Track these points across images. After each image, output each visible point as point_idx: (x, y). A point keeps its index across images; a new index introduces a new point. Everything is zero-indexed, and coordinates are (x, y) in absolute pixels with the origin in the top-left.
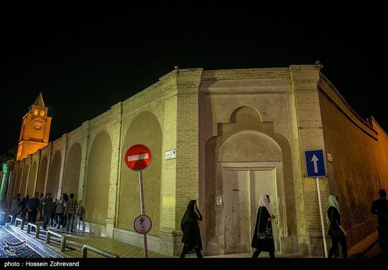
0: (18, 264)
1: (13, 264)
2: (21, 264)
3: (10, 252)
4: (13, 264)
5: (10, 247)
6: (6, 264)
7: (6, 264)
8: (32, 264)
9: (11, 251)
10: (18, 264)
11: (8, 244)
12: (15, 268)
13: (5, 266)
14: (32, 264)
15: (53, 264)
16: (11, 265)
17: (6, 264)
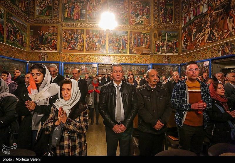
0: (11, 160)
1: (8, 160)
2: (13, 160)
3: (7, 153)
4: (8, 160)
5: (6, 149)
6: (4, 160)
7: (4, 160)
8: (20, 160)
9: (7, 152)
10: (11, 160)
11: (5, 147)
12: (9, 161)
13: (3, 160)
14: (20, 160)
15: (32, 159)
16: (7, 160)
17: (4, 160)
